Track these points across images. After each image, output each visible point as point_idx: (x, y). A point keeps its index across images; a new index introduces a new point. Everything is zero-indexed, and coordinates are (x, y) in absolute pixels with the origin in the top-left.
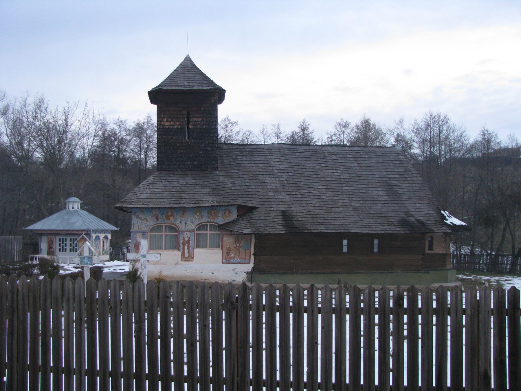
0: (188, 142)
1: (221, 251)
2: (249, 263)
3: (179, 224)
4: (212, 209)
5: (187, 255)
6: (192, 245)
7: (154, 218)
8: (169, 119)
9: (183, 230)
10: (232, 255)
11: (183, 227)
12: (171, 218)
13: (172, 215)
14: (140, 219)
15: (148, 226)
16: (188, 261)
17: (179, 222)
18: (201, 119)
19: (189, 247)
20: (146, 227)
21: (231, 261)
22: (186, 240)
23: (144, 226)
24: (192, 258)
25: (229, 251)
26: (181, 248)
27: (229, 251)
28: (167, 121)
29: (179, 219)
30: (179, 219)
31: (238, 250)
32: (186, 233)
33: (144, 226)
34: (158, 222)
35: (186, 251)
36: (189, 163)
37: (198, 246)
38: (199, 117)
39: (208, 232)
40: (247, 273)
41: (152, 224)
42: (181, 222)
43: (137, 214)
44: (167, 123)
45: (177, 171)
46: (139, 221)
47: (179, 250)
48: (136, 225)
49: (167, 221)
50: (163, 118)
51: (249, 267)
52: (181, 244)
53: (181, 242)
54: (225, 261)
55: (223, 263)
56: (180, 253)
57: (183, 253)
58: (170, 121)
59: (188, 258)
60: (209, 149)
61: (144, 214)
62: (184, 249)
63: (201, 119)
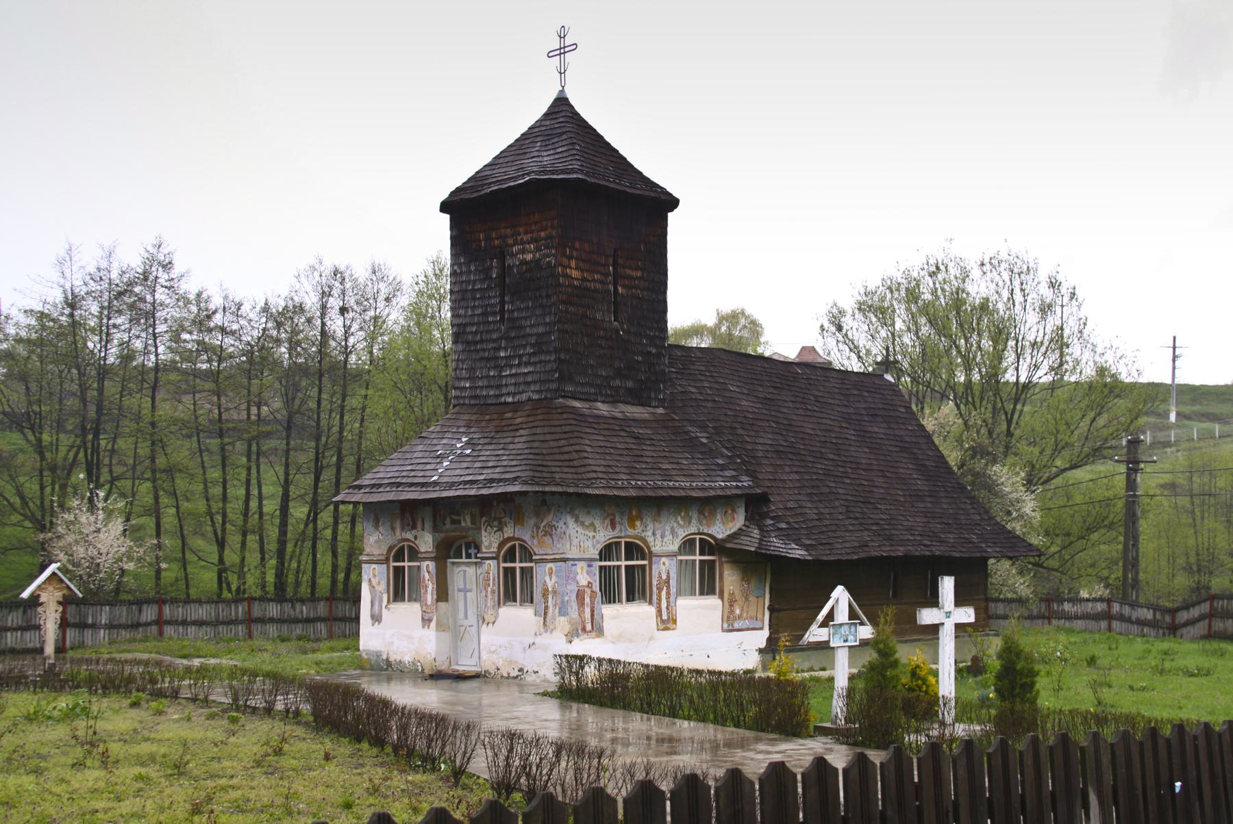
0: (617, 331)
1: (720, 602)
2: (762, 629)
3: (650, 539)
4: (708, 505)
5: (665, 617)
6: (673, 590)
7: (607, 522)
8: (582, 265)
9: (659, 553)
10: (738, 612)
11: (657, 547)
12: (638, 523)
13: (640, 517)
14: (582, 524)
15: (598, 542)
16: (666, 629)
17: (650, 533)
18: (639, 274)
19: (668, 593)
20: (594, 546)
21: (736, 626)
22: (664, 577)
23: (589, 543)
24: (675, 622)
25: (732, 603)
26: (655, 597)
27: (732, 603)
28: (577, 268)
29: (650, 526)
30: (650, 526)
31: (747, 599)
32: (663, 559)
33: (589, 543)
34: (616, 533)
35: (664, 605)
36: (618, 383)
37: (679, 593)
38: (637, 269)
39: (698, 558)
40: (761, 651)
41: (603, 539)
42: (654, 534)
43: (576, 512)
44: (575, 274)
45: (596, 401)
46: (580, 530)
47: (651, 603)
48: (575, 541)
49: (631, 532)
50: (570, 258)
51: (761, 638)
52: (655, 589)
53: (655, 583)
54: (725, 626)
55: (723, 630)
56: (652, 610)
57: (659, 611)
58: (582, 271)
59: (667, 622)
60: (654, 351)
61: (588, 513)
62: (660, 600)
63: (639, 274)
